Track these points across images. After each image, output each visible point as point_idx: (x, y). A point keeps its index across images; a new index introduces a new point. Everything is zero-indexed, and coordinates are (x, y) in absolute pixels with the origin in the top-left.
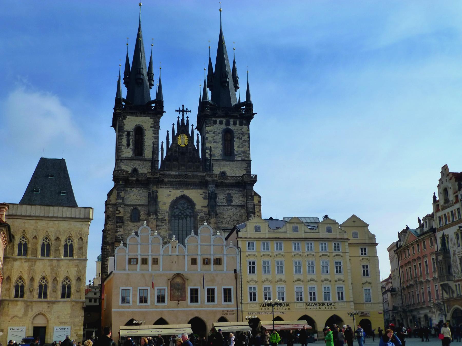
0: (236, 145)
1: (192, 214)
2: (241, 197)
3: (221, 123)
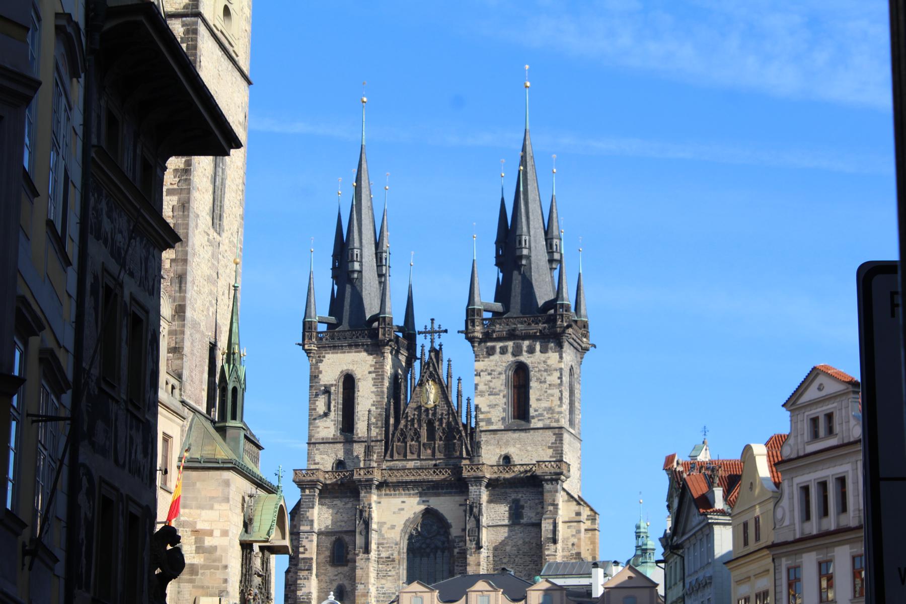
0: (533, 395)
1: (446, 545)
2: (540, 506)
3: (504, 351)
